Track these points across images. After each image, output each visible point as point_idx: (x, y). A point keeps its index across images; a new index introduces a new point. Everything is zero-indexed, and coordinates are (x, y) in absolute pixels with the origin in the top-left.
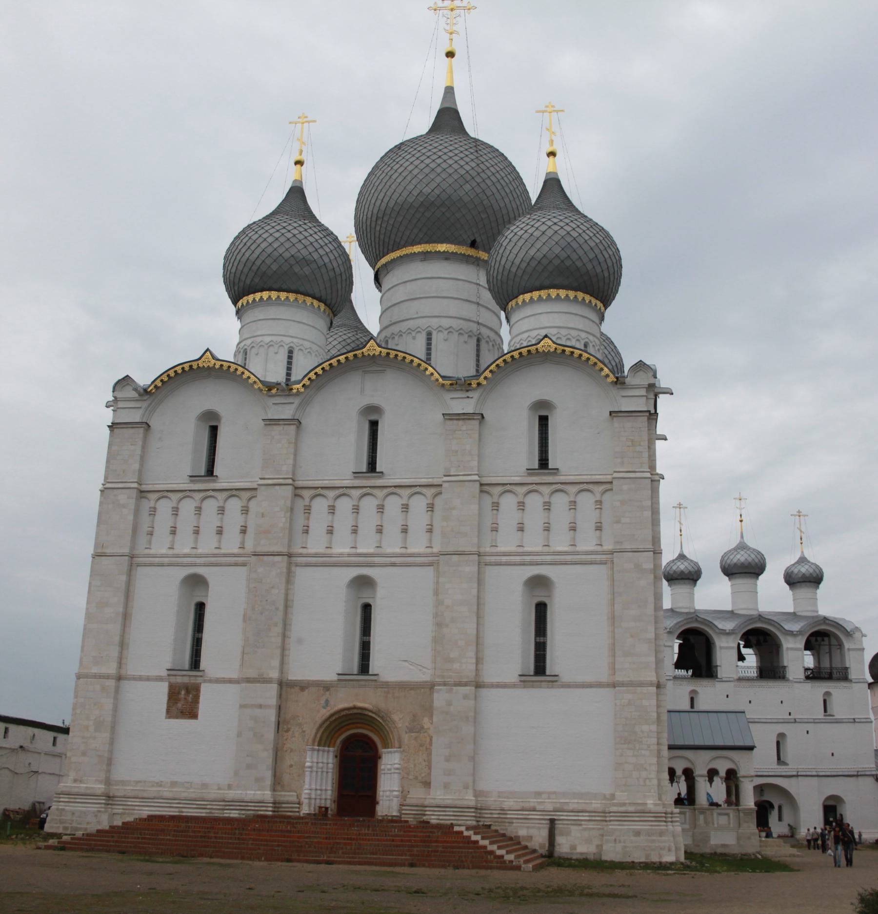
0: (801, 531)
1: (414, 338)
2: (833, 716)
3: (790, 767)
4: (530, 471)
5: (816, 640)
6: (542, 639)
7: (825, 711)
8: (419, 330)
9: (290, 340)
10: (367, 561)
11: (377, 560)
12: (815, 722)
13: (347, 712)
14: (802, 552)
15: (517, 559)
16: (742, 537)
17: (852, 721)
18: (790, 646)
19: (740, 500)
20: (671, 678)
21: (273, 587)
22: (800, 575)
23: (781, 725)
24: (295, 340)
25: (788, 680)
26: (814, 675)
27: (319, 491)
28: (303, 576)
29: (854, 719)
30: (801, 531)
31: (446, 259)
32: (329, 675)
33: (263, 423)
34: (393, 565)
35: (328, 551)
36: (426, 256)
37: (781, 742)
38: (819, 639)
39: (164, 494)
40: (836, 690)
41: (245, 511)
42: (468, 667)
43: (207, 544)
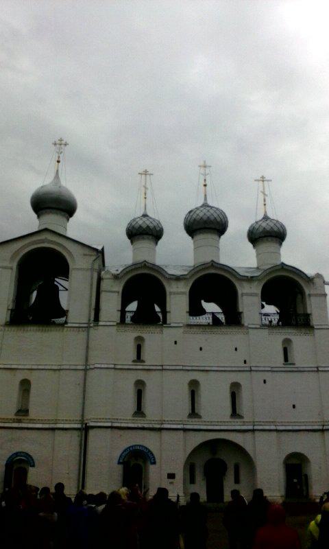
0: (264, 194)
2: (294, 364)
3: (245, 420)
7: (286, 359)
14: (266, 212)
16: (206, 199)
17: (316, 369)
18: (245, 291)
19: (205, 167)
20: (115, 324)
22: (261, 230)
23: (234, 374)
25: (243, 325)
29: (317, 367)
30: (264, 194)
37: (236, 392)
40: (300, 341)
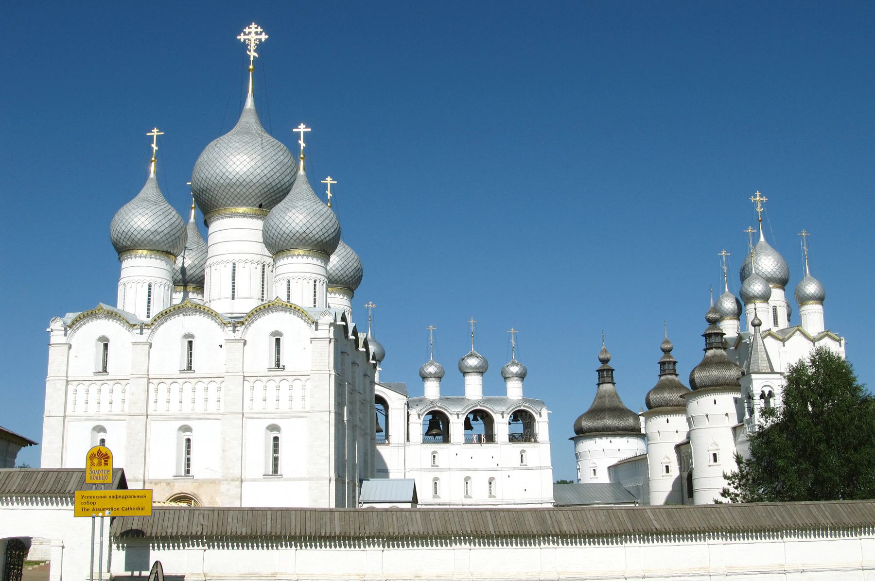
1: (225, 266)
4: (270, 369)
5: (521, 415)
6: (275, 455)
7: (522, 462)
8: (228, 261)
9: (150, 278)
10: (187, 416)
11: (192, 417)
12: (514, 469)
13: (179, 495)
15: (262, 416)
21: (139, 432)
24: (153, 278)
26: (513, 438)
27: (161, 380)
28: (154, 426)
31: (244, 217)
32: (169, 476)
33: (131, 344)
34: (200, 419)
35: (167, 412)
36: (232, 215)
38: (524, 414)
39: (80, 382)
41: (124, 391)
42: (236, 472)
43: (105, 408)
